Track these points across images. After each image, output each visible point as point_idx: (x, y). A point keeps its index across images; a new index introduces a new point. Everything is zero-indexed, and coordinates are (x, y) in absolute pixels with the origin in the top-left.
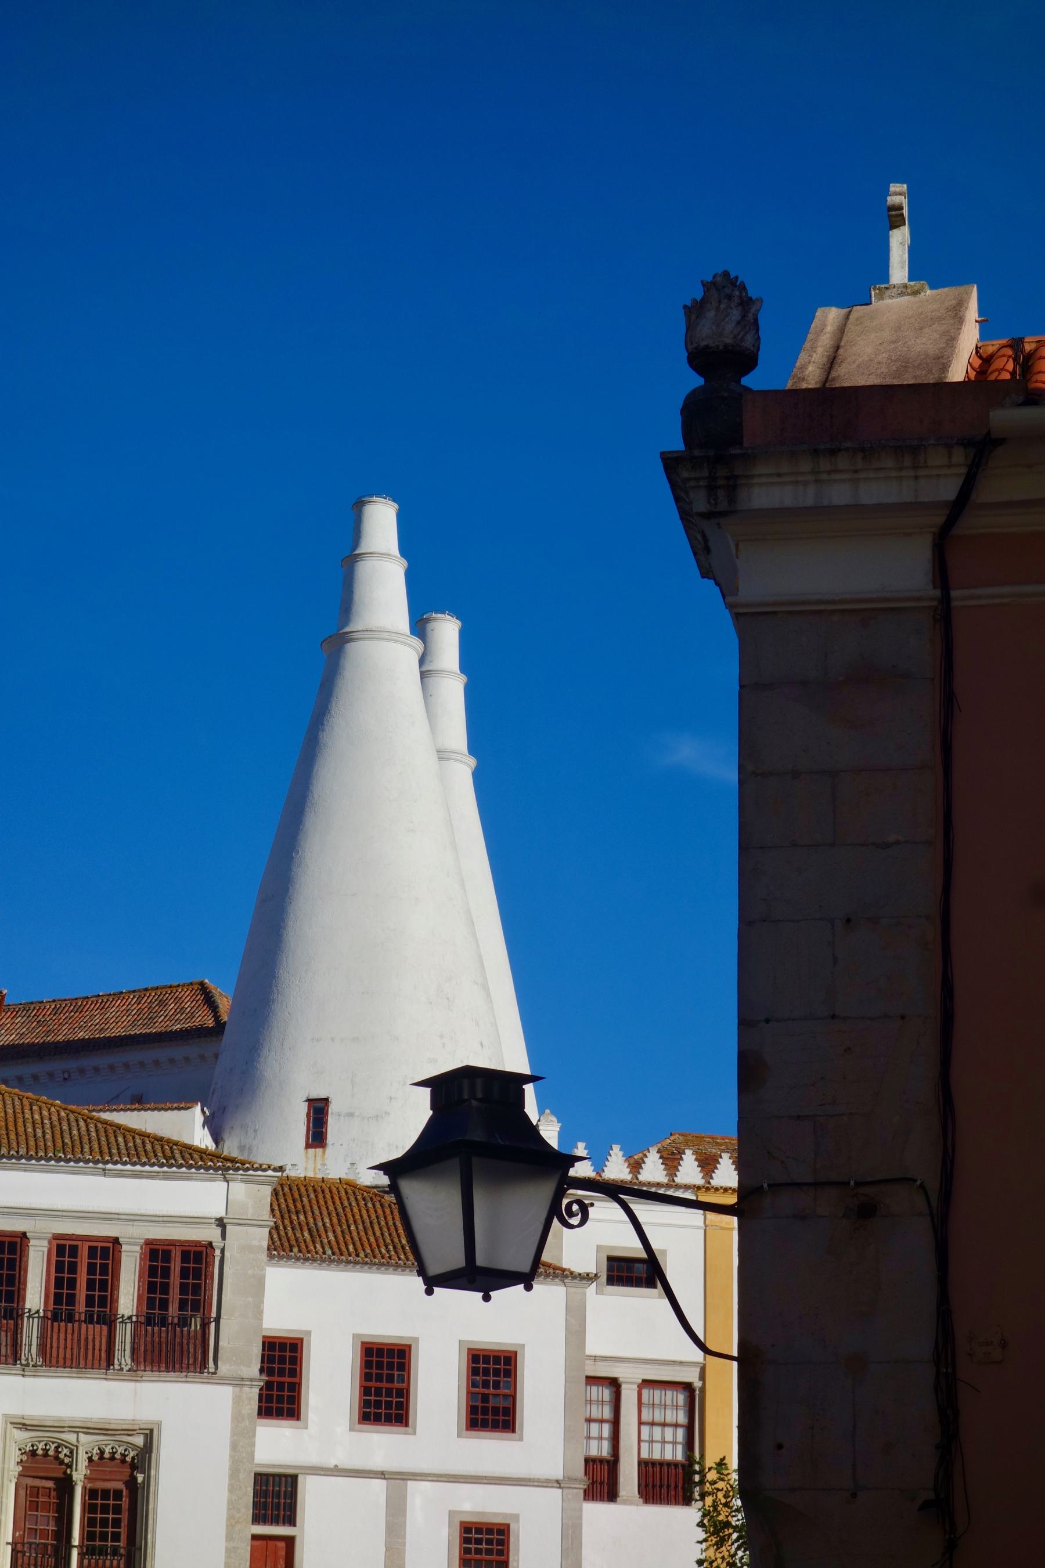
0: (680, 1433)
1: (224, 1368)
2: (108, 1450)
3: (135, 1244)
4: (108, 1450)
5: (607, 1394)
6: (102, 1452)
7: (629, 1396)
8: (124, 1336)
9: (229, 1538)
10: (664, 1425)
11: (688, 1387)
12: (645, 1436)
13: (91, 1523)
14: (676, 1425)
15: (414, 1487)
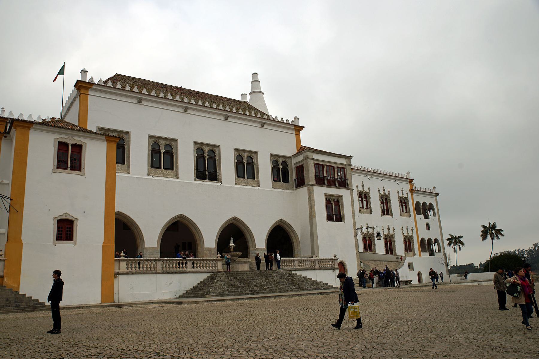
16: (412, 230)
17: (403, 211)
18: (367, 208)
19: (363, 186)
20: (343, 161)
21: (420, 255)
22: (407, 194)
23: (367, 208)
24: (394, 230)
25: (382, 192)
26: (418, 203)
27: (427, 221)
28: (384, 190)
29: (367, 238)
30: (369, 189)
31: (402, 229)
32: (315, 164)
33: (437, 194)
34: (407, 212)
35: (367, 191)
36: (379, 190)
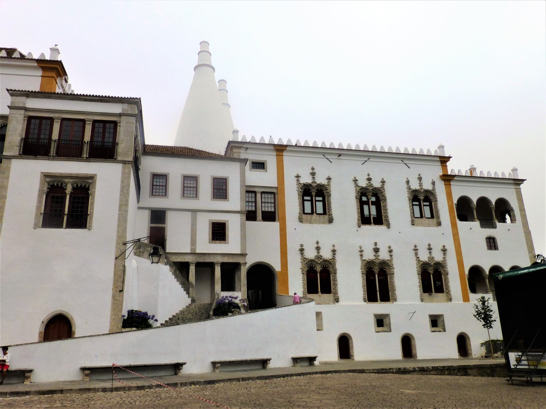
0: (273, 205)
1: (119, 158)
2: (79, 185)
3: (90, 121)
4: (79, 185)
5: (253, 195)
6: (78, 185)
7: (259, 196)
8: (86, 149)
9: (120, 210)
10: (268, 203)
11: (274, 193)
12: (263, 205)
13: (73, 207)
14: (271, 203)
15: (198, 213)
16: (444, 250)
17: (422, 217)
18: (325, 213)
19: (313, 174)
20: (116, 109)
21: (466, 299)
22: (433, 183)
23: (325, 213)
24: (391, 251)
25: (363, 183)
26: (464, 202)
27: (489, 232)
28: (369, 179)
29: (318, 269)
30: (329, 179)
31: (416, 250)
32: (30, 118)
33: (518, 182)
34: (432, 217)
35: (324, 182)
36: (355, 181)
